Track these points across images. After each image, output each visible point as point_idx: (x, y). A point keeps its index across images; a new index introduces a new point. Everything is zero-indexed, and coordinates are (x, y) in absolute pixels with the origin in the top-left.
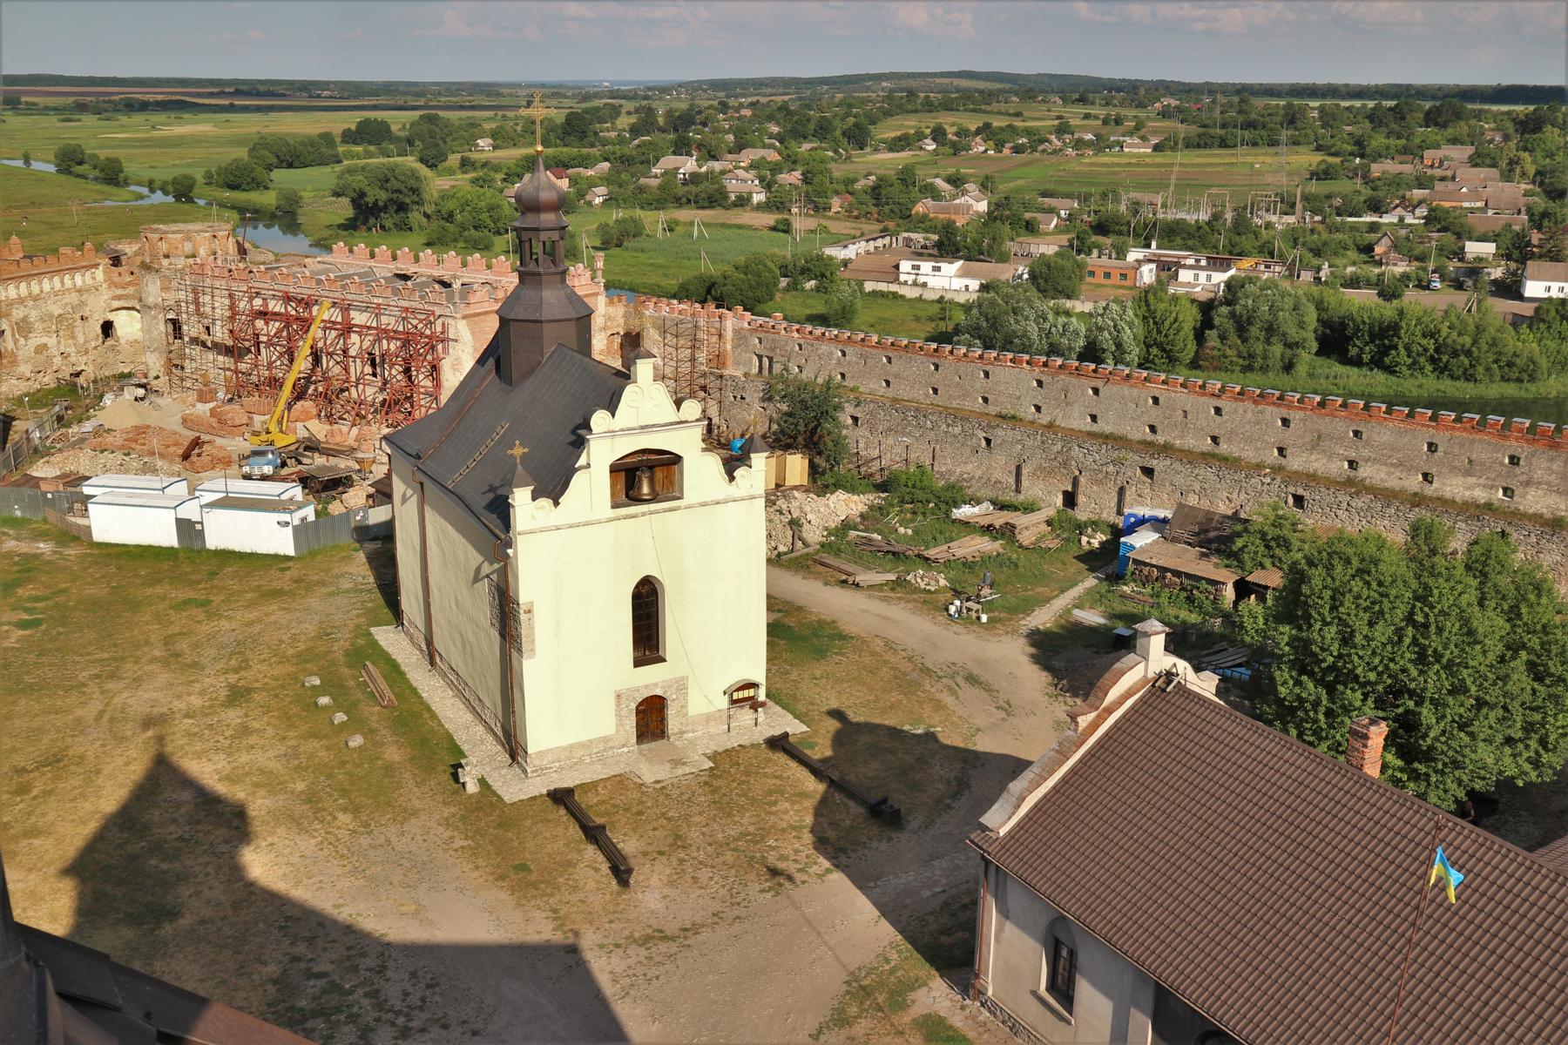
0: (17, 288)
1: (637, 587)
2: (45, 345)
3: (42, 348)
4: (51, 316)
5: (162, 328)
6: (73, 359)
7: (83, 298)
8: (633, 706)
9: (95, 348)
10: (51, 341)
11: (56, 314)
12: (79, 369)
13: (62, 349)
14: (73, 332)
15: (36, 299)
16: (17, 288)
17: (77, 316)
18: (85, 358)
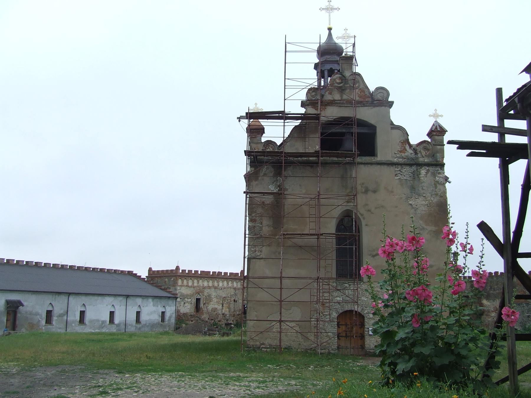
0: (208, 282)
2: (217, 308)
3: (215, 310)
4: (221, 297)
6: (227, 317)
7: (237, 291)
8: (335, 315)
9: (238, 315)
10: (220, 307)
11: (224, 296)
12: (230, 322)
13: (223, 311)
14: (229, 306)
15: (216, 288)
16: (208, 282)
17: (232, 299)
18: (233, 318)
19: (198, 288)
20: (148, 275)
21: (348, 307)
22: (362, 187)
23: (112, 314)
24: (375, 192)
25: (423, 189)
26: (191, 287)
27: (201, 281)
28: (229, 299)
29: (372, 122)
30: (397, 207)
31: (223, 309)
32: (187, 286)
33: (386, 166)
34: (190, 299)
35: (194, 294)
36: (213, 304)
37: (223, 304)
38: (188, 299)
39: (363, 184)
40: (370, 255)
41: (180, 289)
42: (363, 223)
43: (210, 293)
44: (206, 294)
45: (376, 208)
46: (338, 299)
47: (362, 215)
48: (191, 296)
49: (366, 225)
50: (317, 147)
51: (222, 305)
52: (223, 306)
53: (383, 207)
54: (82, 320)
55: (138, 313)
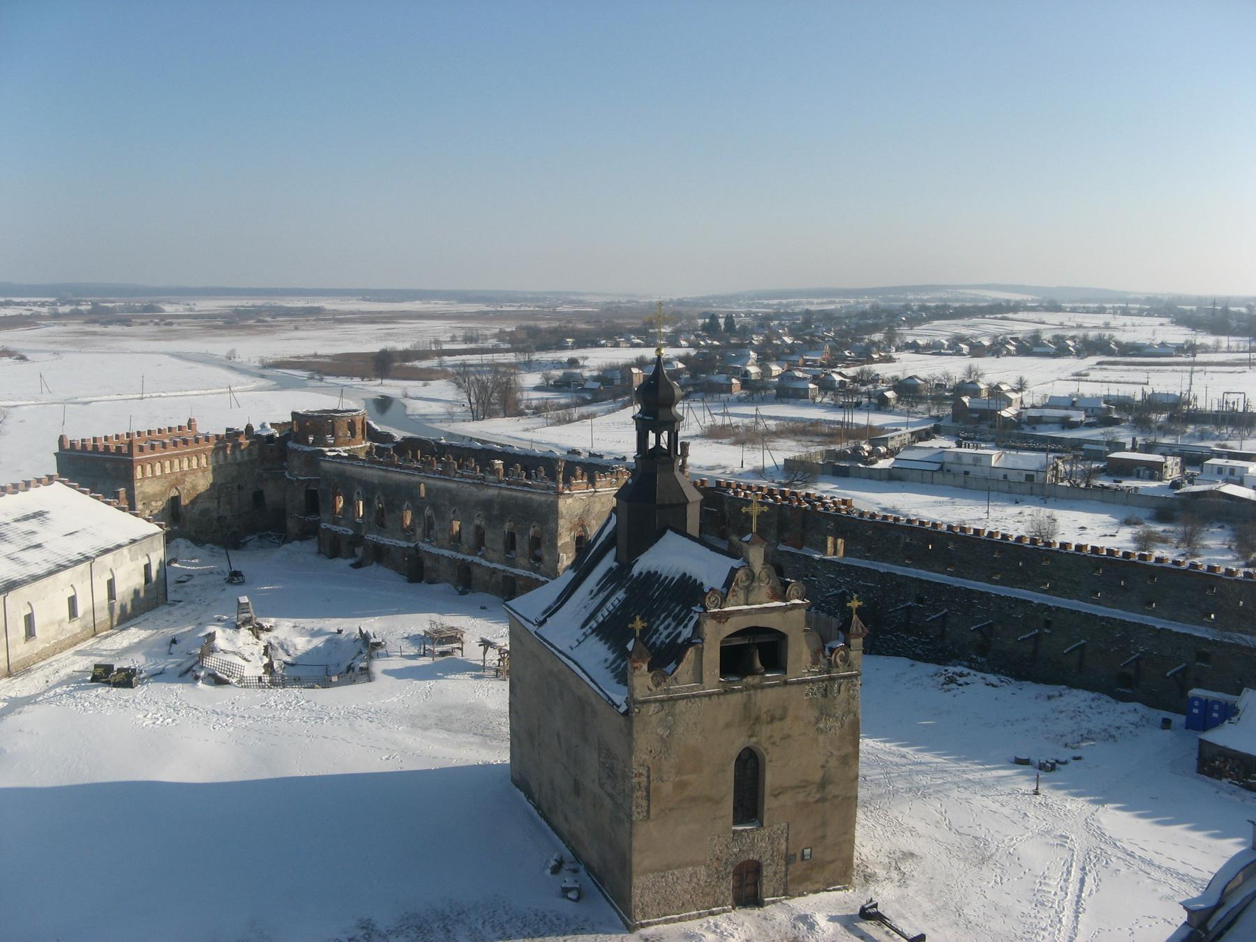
1: (740, 754)
2: (208, 509)
5: (302, 497)
8: (730, 869)
19: (173, 477)
20: (58, 451)
21: (744, 858)
22: (767, 715)
23: (72, 601)
24: (782, 719)
25: (835, 708)
26: (160, 477)
27: (176, 462)
28: (230, 485)
29: (782, 630)
30: (805, 734)
31: (219, 506)
32: (154, 476)
33: (796, 686)
34: (161, 500)
35: (166, 489)
36: (202, 502)
37: (219, 498)
38: (156, 501)
39: (769, 711)
40: (772, 795)
41: (141, 486)
42: (767, 758)
43: (195, 483)
44: (188, 485)
45: (782, 739)
46: (735, 850)
47: (766, 750)
48: (163, 493)
49: (770, 761)
50: (717, 671)
51: (216, 501)
52: (219, 502)
53: (789, 736)
54: (30, 633)
55: (111, 584)
